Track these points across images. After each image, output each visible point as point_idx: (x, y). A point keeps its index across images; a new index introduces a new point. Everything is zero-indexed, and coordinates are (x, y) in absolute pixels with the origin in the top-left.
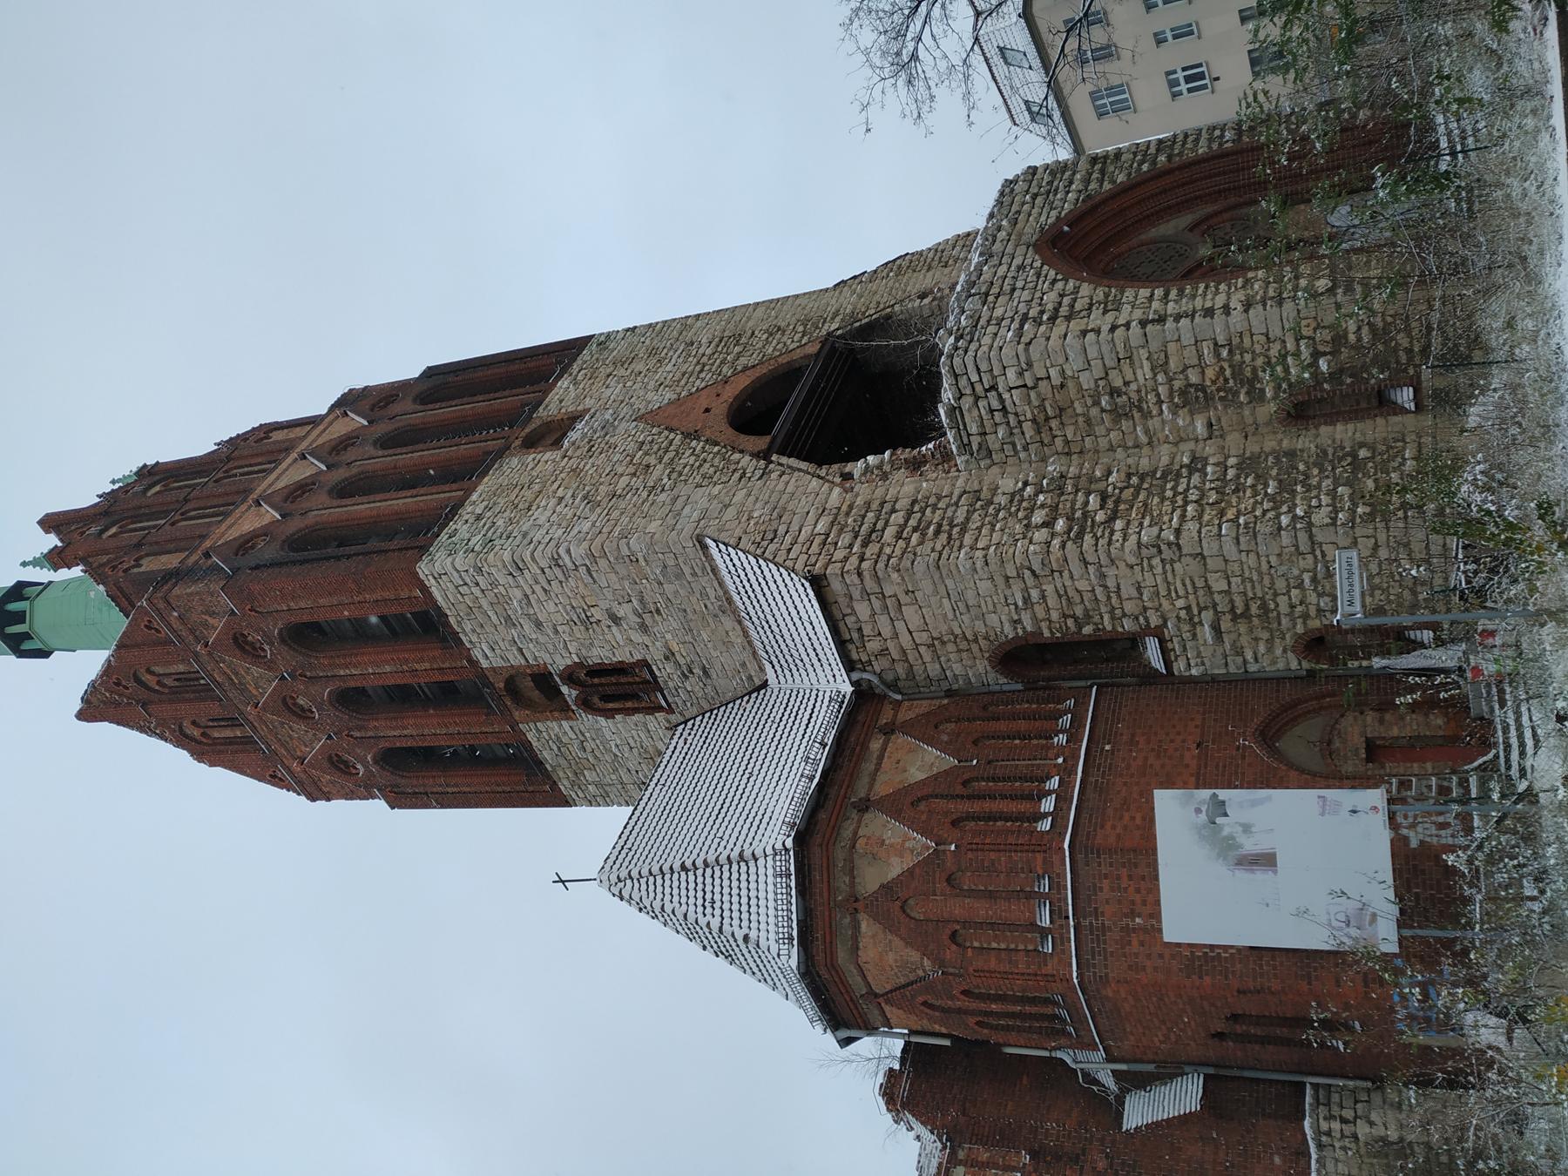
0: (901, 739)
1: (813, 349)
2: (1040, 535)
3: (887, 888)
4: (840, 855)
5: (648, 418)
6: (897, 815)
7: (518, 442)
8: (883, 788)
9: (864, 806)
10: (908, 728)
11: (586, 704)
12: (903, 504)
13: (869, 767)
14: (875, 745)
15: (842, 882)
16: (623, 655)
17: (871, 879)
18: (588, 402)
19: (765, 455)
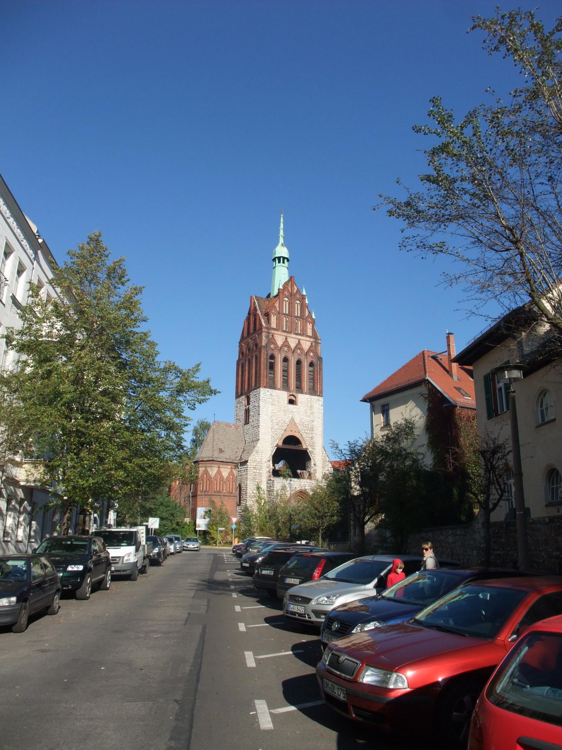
0: (230, 470)
1: (304, 447)
2: (251, 492)
3: (208, 471)
4: (212, 465)
5: (292, 419)
6: (217, 472)
7: (291, 393)
8: (221, 469)
9: (219, 467)
10: (231, 471)
11: (246, 410)
12: (261, 471)
13: (225, 466)
14: (229, 467)
15: (209, 465)
16: (250, 420)
17: (209, 469)
19: (277, 445)
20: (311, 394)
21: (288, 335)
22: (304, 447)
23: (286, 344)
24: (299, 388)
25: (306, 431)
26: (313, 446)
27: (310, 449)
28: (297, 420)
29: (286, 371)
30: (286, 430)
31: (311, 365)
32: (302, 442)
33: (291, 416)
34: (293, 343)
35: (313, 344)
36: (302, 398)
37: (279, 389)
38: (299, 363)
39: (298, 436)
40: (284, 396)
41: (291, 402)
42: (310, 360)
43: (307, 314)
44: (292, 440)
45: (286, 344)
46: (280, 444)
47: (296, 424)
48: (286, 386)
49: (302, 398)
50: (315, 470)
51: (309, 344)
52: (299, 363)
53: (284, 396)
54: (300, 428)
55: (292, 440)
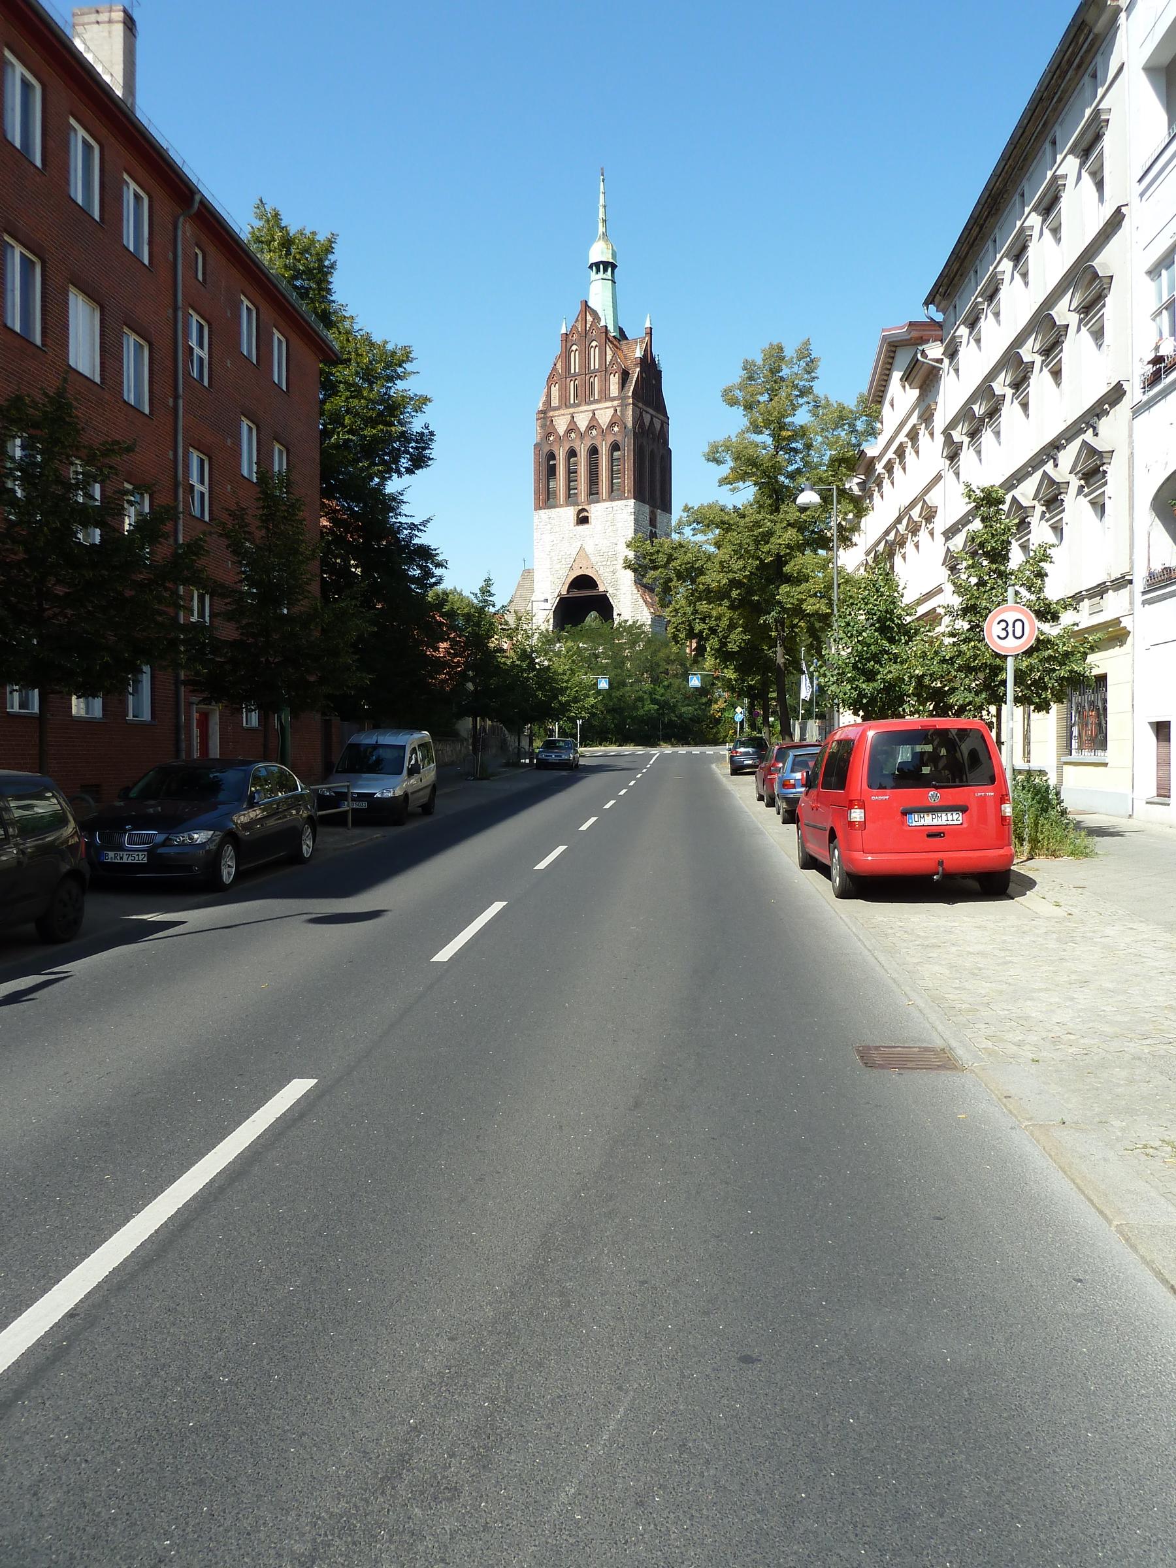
20: (612, 499)
21: (577, 409)
22: (601, 589)
27: (611, 591)
28: (589, 549)
29: (571, 473)
34: (582, 423)
36: (596, 511)
37: (561, 506)
38: (594, 451)
40: (570, 513)
41: (583, 520)
42: (610, 439)
44: (584, 582)
46: (564, 592)
48: (571, 498)
52: (594, 451)
54: (594, 559)
55: (584, 582)
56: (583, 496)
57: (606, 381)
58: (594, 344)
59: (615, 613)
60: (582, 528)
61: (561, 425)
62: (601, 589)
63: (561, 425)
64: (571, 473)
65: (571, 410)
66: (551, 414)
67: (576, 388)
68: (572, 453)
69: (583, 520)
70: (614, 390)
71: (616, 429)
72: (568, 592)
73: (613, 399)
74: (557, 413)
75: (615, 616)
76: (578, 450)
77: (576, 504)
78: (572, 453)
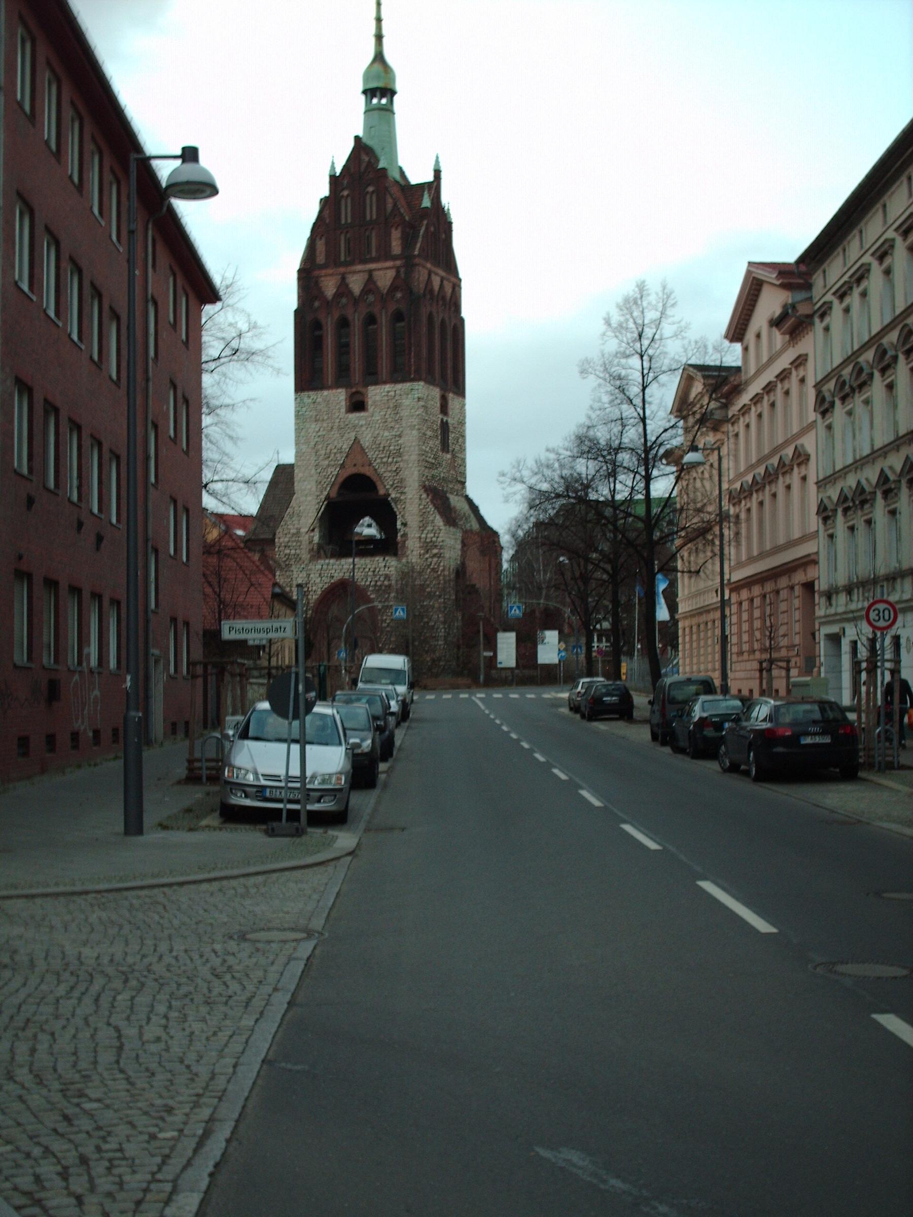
7: (354, 390)
18: (371, 409)
19: (328, 498)
22: (382, 492)
23: (343, 289)
24: (372, 376)
25: (385, 460)
26: (400, 485)
30: (342, 466)
31: (398, 316)
32: (378, 484)
33: (352, 435)
34: (356, 284)
35: (402, 270)
39: (367, 471)
40: (339, 396)
42: (392, 307)
43: (389, 206)
45: (343, 289)
46: (334, 494)
47: (363, 449)
48: (342, 378)
49: (376, 394)
50: (405, 535)
51: (391, 274)
52: (371, 320)
53: (339, 396)
56: (357, 376)
57: (388, 235)
58: (371, 189)
59: (399, 523)
60: (353, 416)
61: (329, 287)
62: (382, 492)
63: (329, 287)
64: (343, 349)
65: (342, 270)
66: (316, 273)
67: (348, 241)
68: (344, 323)
69: (357, 405)
70: (396, 247)
71: (399, 295)
72: (339, 493)
73: (394, 258)
74: (323, 272)
75: (399, 527)
76: (350, 318)
77: (347, 386)
78: (344, 323)
